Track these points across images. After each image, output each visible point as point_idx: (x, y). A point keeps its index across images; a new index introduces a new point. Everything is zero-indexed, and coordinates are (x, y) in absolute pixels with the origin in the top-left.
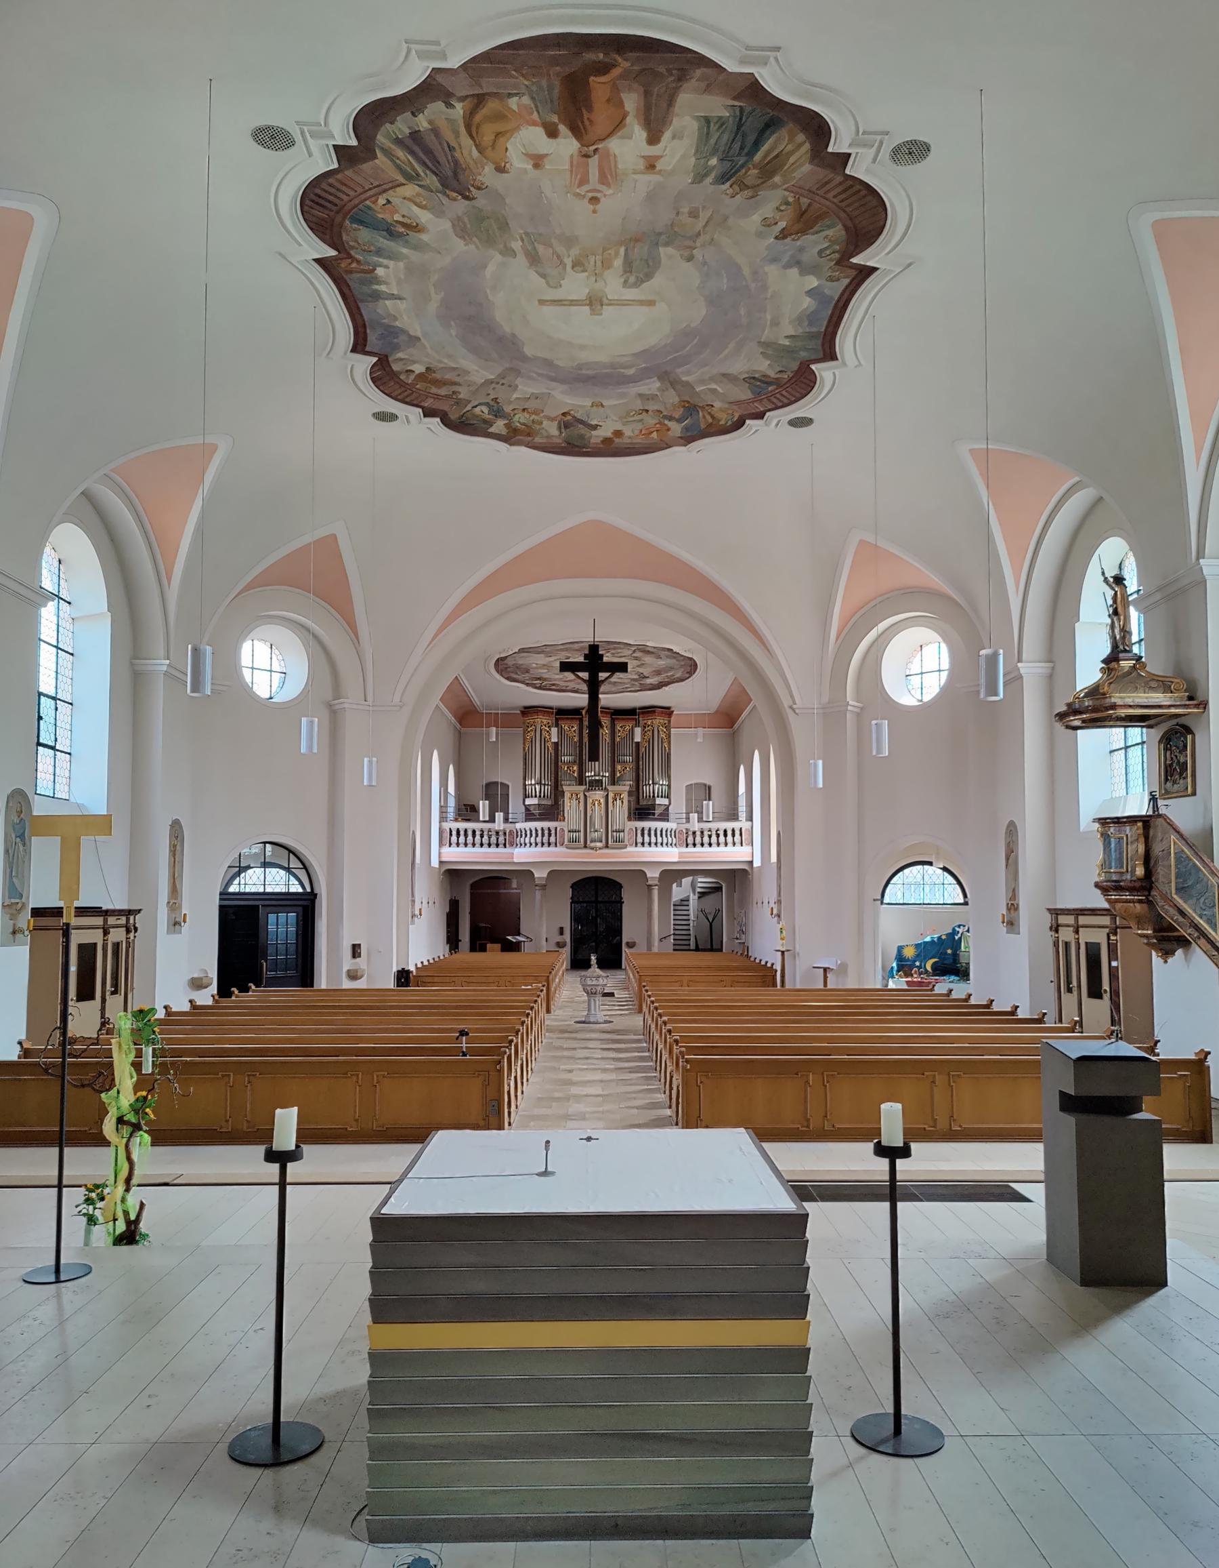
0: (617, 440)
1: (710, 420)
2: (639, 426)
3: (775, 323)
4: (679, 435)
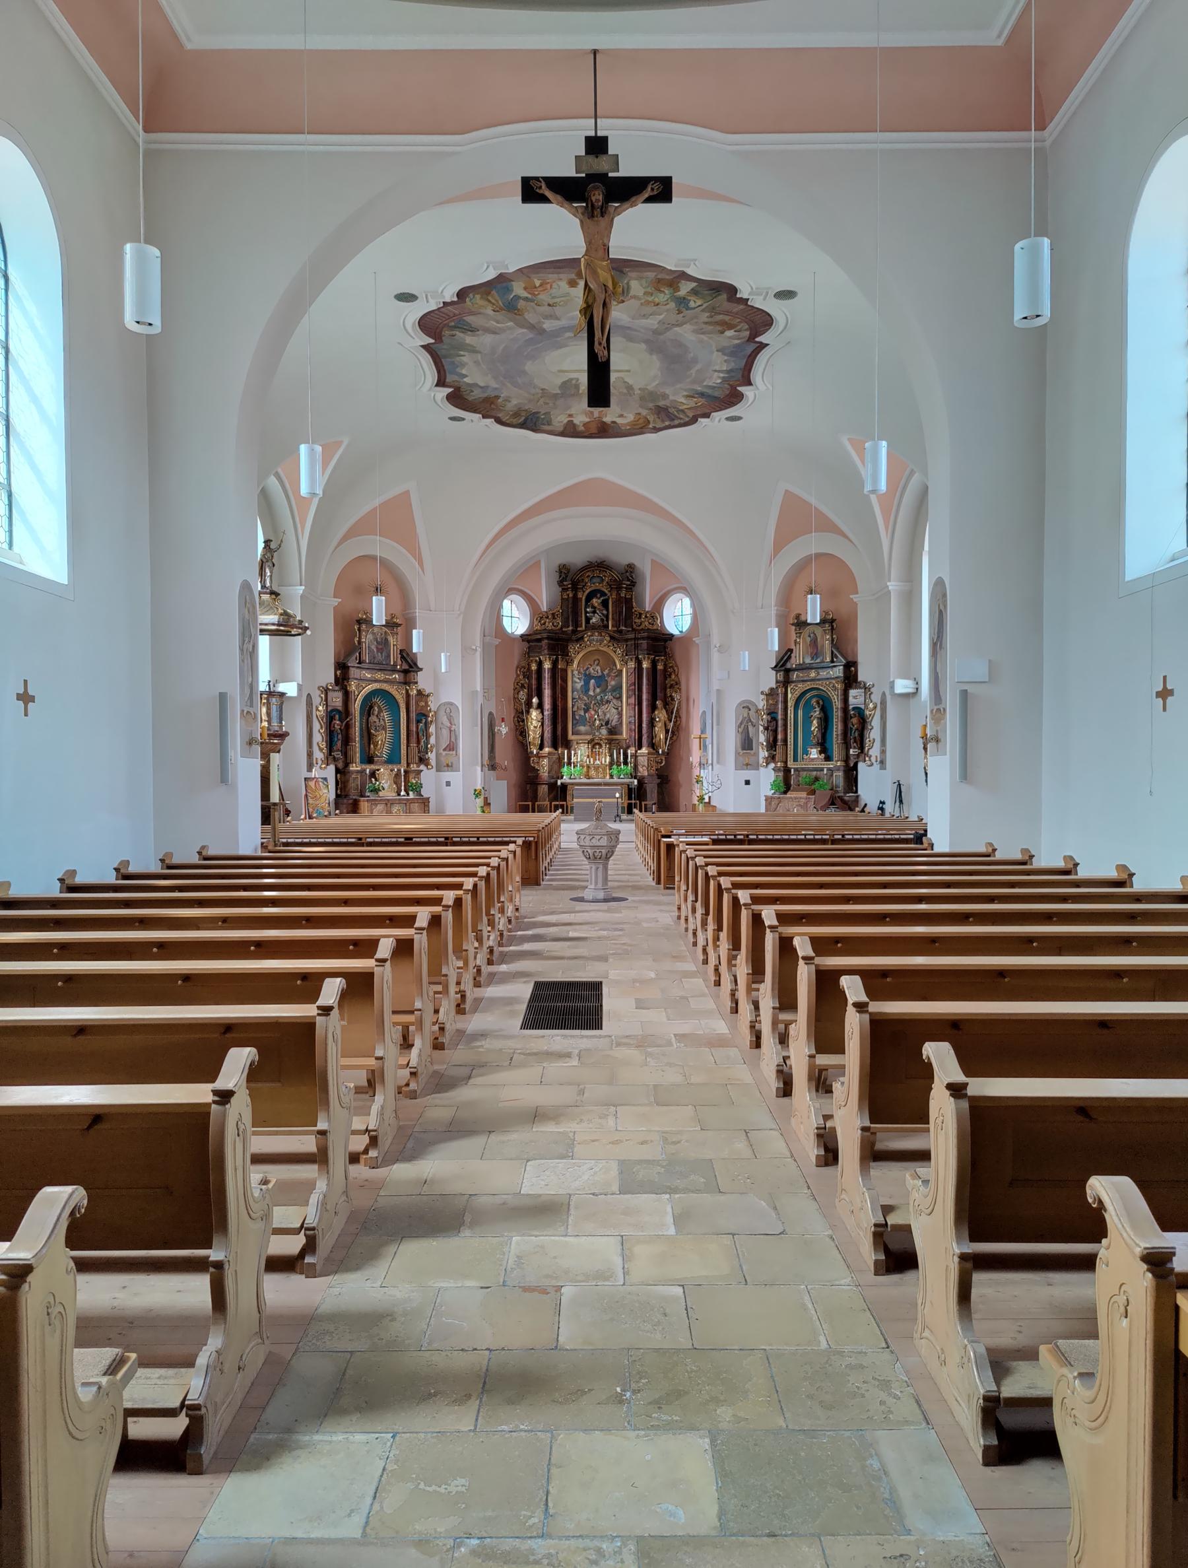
0: (573, 276)
1: (490, 298)
2: (553, 291)
3: (477, 363)
4: (513, 283)
